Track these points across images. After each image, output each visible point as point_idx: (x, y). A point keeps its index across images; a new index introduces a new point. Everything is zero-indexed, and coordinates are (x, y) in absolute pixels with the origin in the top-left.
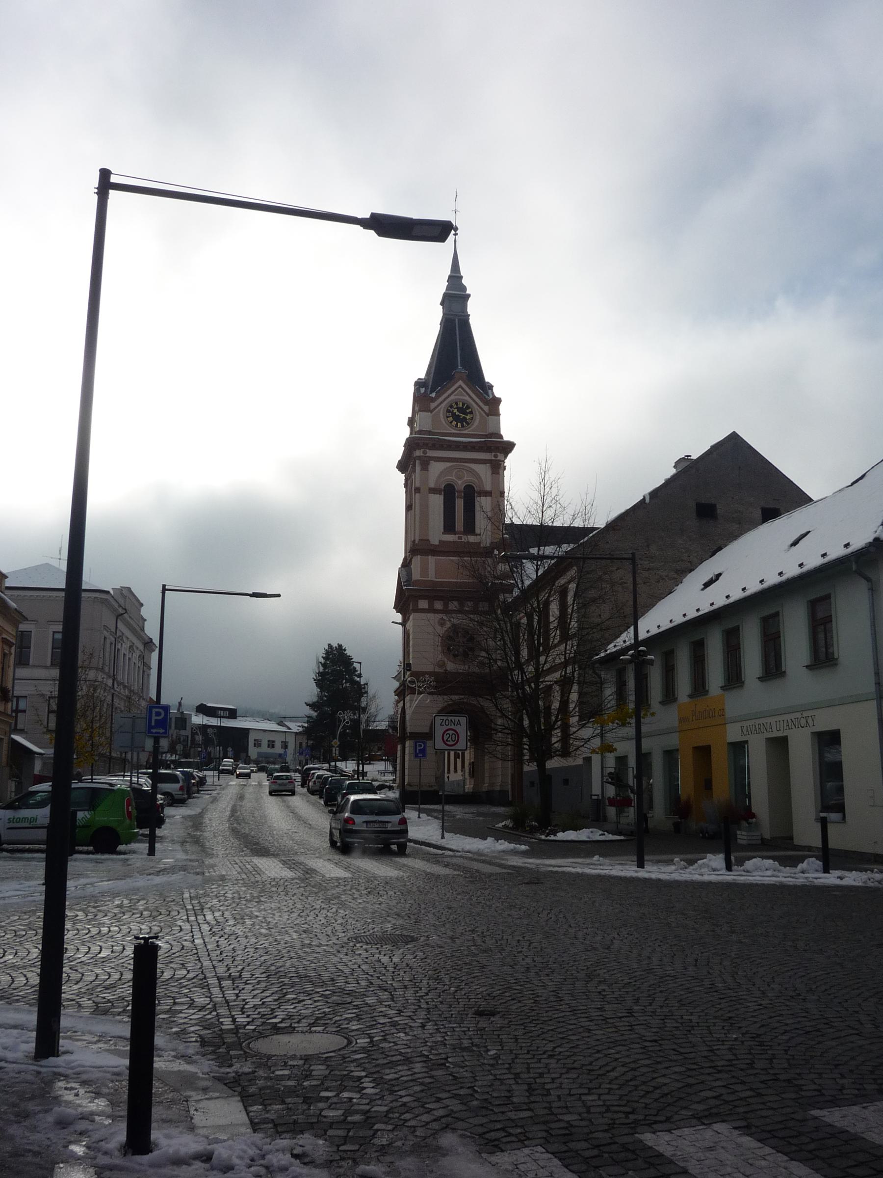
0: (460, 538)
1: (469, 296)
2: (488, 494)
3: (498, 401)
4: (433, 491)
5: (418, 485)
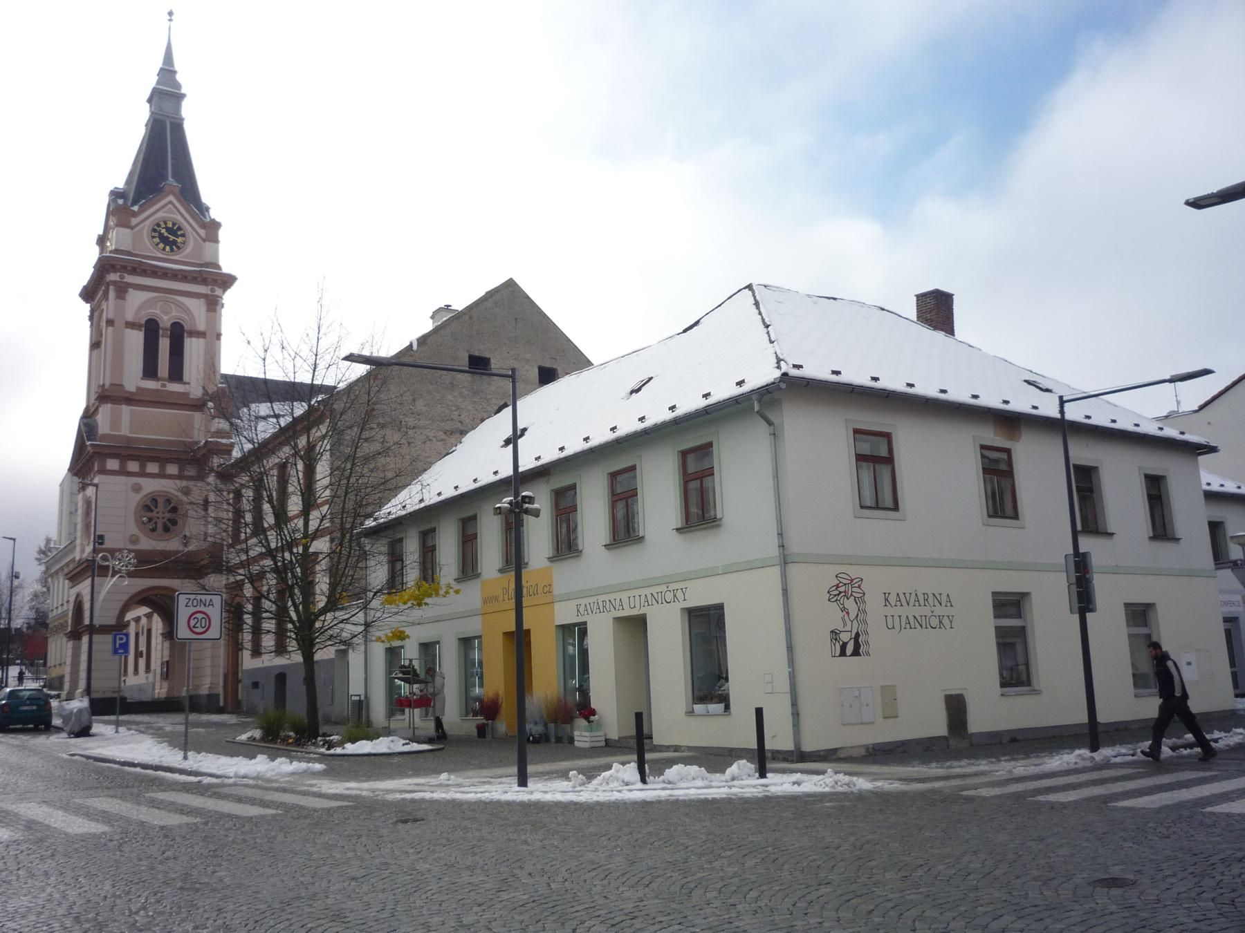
0: (164, 386)
1: (183, 96)
2: (201, 335)
3: (215, 226)
4: (131, 325)
5: (111, 316)
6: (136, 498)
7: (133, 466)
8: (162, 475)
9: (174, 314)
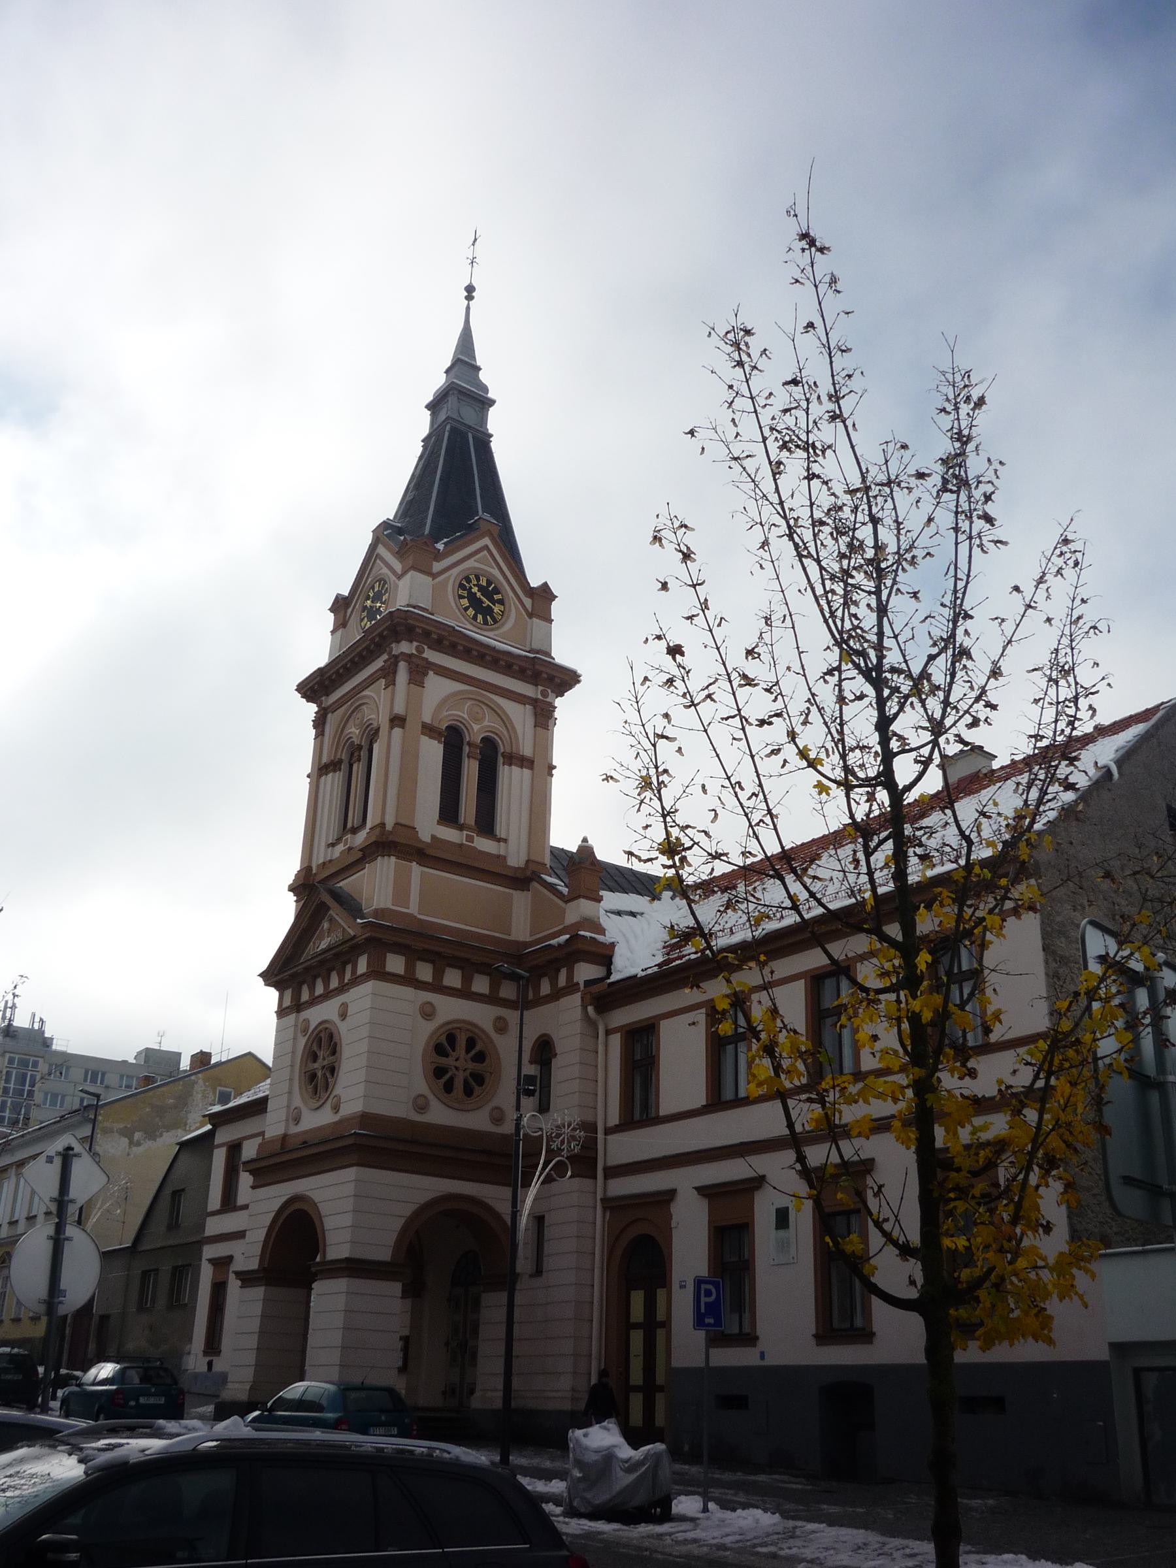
2: (526, 762)
3: (544, 596)
4: (429, 730)
5: (399, 709)
6: (426, 1030)
7: (425, 972)
8: (465, 993)
9: (486, 723)
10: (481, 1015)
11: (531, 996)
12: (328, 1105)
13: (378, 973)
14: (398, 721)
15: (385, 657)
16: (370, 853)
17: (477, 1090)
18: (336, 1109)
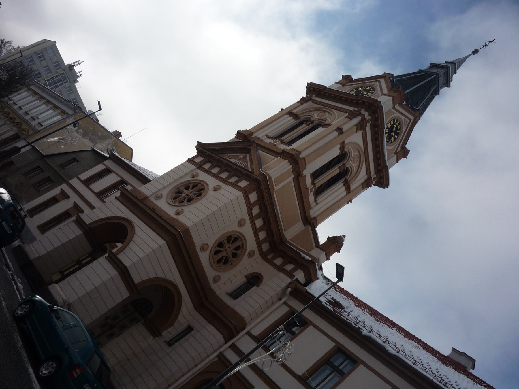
2: (348, 190)
4: (343, 145)
5: (345, 128)
7: (256, 211)
8: (256, 232)
9: (354, 165)
10: (251, 244)
11: (269, 257)
12: (177, 208)
13: (246, 193)
14: (340, 130)
15: (357, 109)
16: (284, 154)
17: (222, 264)
18: (178, 213)
